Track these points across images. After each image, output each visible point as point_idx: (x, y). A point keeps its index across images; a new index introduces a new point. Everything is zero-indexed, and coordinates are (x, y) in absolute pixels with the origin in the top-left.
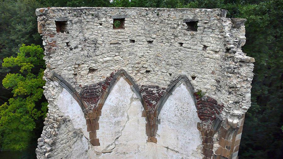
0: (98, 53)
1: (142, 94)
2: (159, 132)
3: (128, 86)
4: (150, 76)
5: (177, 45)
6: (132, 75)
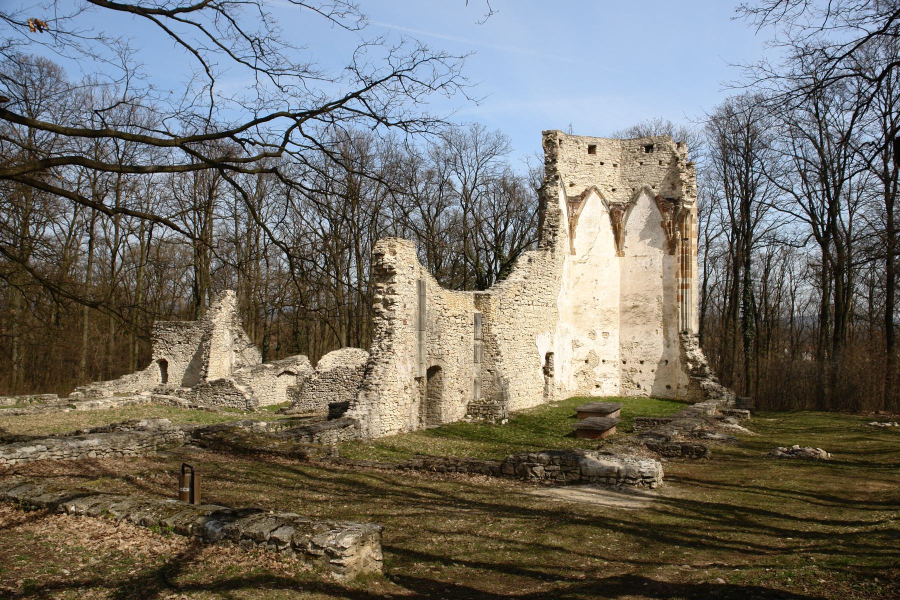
0: (577, 170)
1: (611, 207)
2: (625, 245)
3: (599, 200)
4: (615, 194)
5: (639, 165)
6: (602, 191)
